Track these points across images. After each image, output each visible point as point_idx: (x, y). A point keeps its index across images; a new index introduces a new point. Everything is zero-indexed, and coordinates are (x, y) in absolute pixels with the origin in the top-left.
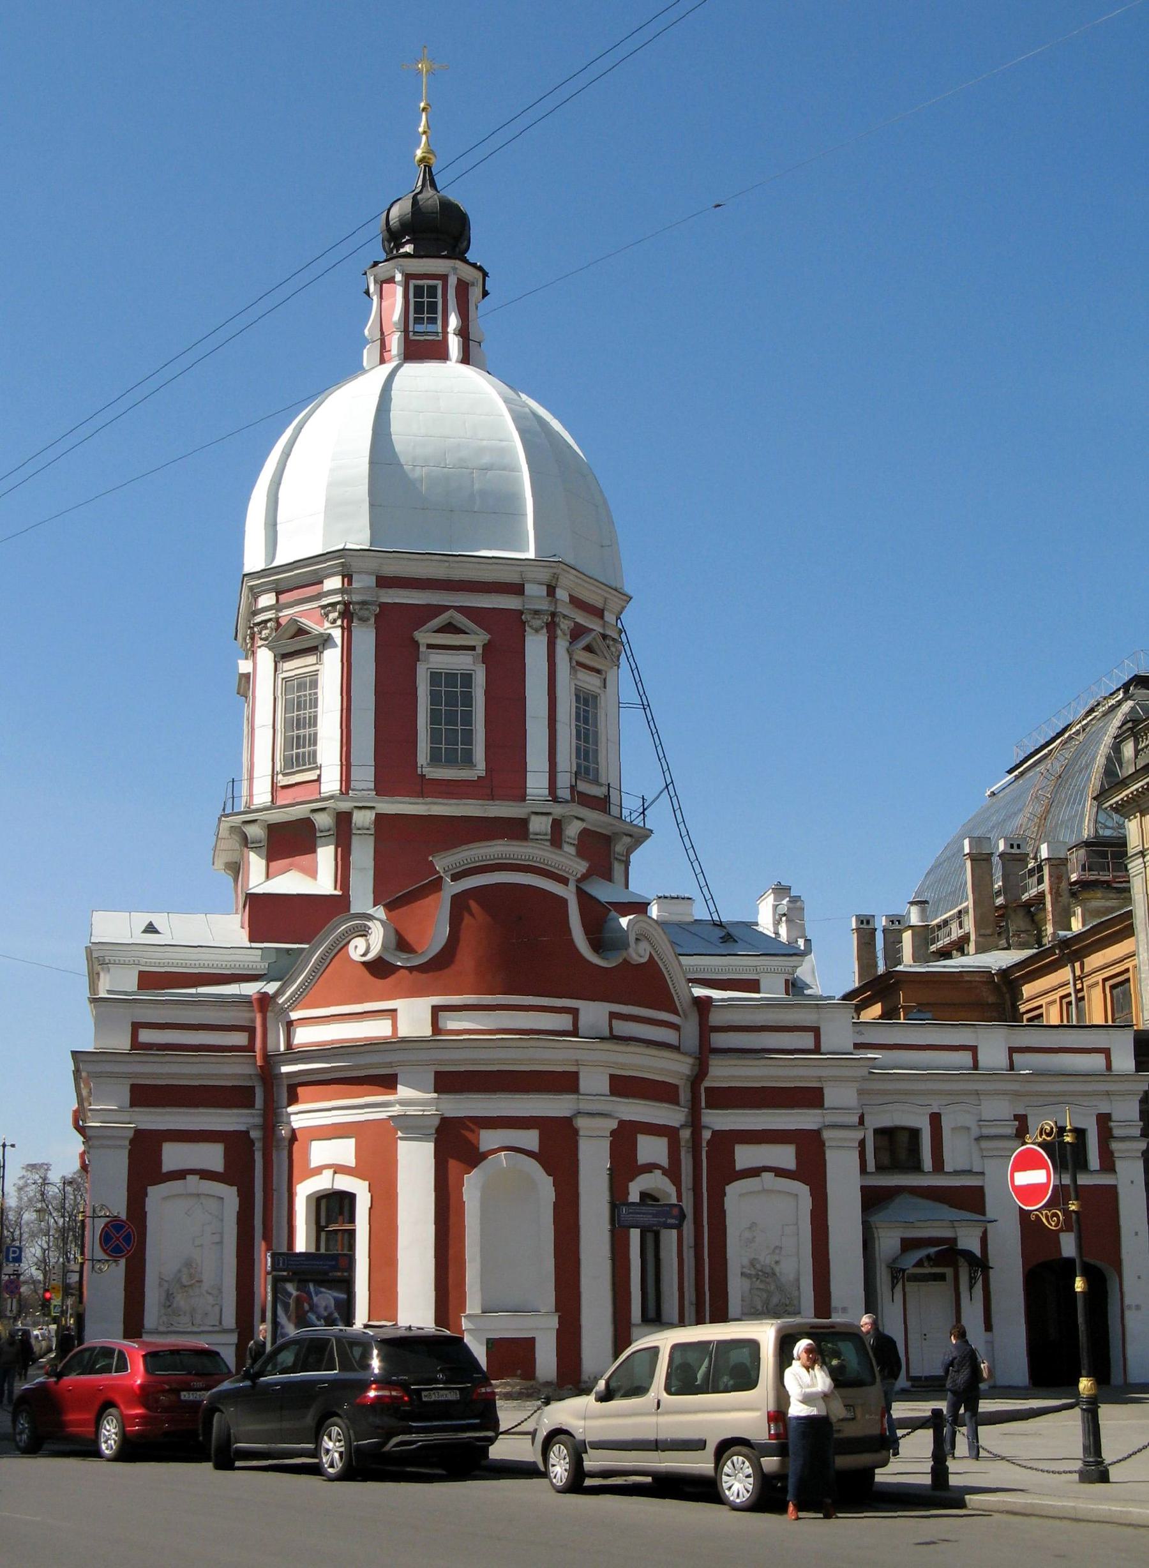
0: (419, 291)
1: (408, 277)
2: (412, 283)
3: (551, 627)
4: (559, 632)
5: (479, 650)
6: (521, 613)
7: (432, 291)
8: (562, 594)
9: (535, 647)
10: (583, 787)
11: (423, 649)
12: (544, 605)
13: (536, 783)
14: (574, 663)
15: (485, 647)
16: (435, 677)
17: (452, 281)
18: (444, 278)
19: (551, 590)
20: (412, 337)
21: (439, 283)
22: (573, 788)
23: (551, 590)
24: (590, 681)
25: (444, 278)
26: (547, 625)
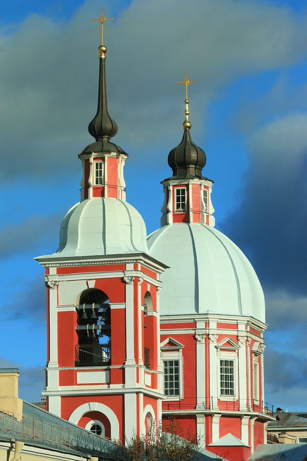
0: (178, 191)
1: (174, 186)
2: (176, 189)
5: (181, 350)
7: (183, 191)
8: (213, 325)
9: (200, 348)
12: (204, 332)
13: (201, 399)
14: (219, 350)
16: (165, 363)
18: (187, 186)
22: (219, 400)
23: (207, 324)
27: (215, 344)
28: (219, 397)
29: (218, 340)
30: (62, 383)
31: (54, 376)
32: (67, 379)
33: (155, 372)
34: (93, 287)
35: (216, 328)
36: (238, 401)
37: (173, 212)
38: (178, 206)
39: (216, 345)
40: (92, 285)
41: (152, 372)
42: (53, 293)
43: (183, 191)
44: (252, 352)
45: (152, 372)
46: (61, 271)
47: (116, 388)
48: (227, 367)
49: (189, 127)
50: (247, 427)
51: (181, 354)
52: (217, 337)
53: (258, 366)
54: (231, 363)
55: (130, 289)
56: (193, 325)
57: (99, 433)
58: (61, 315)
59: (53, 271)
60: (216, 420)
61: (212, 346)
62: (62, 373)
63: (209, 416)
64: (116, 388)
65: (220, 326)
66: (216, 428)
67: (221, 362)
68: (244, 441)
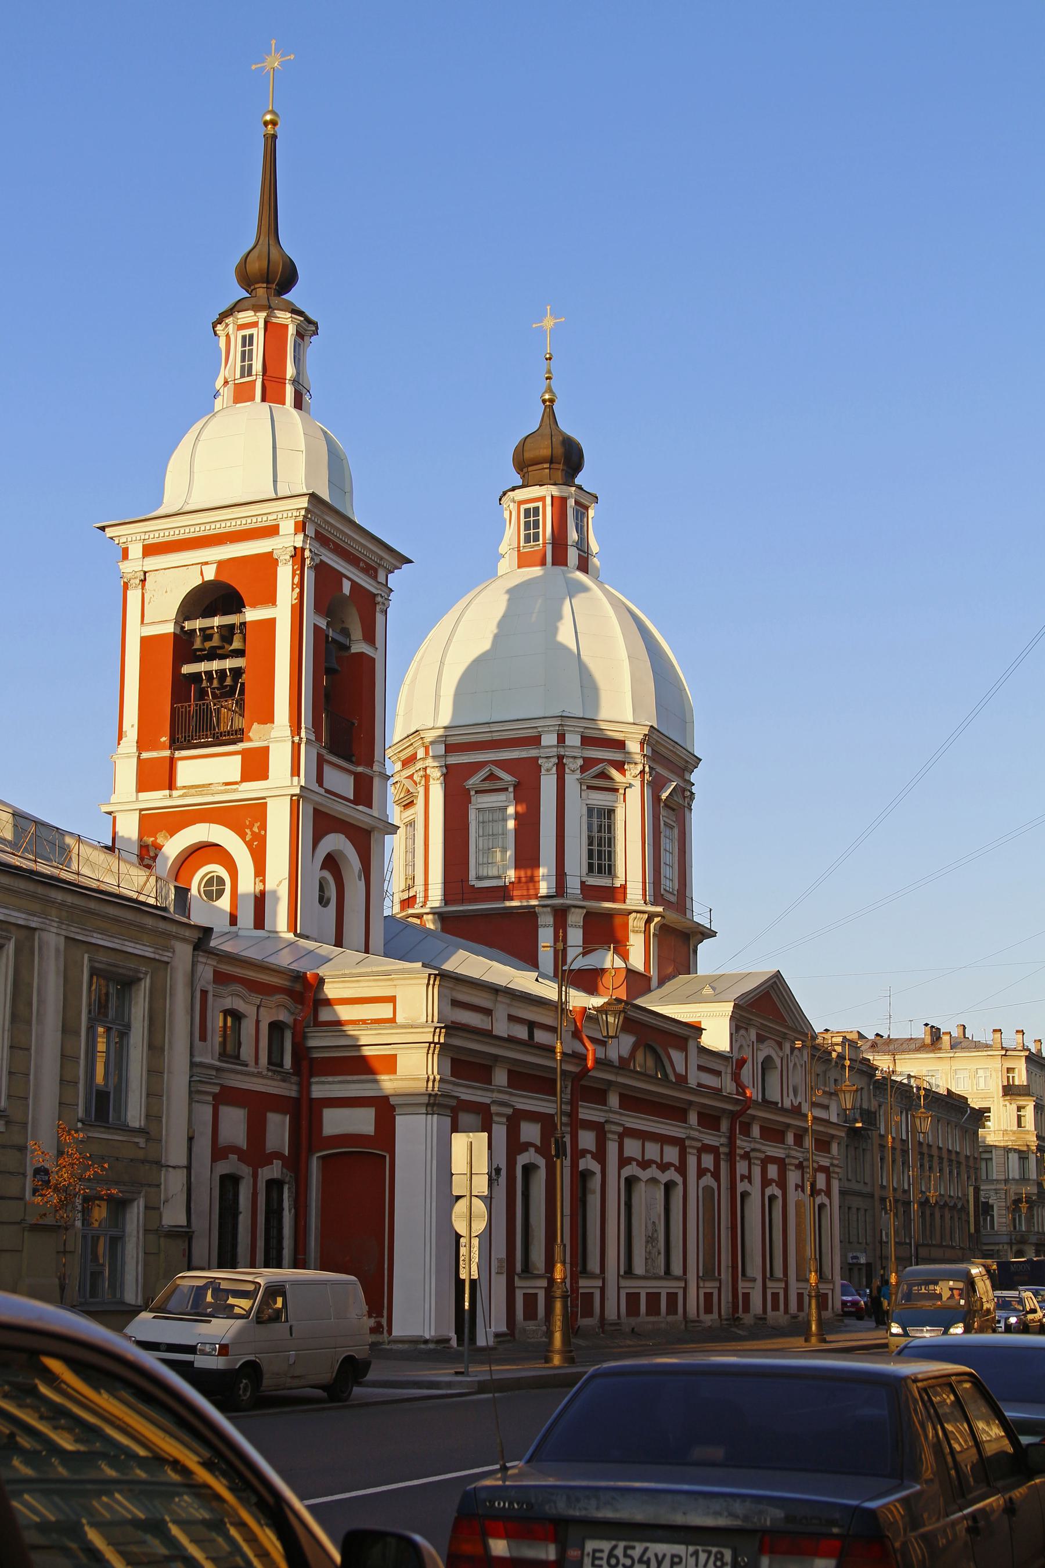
0: (527, 512)
2: (523, 507)
3: (561, 767)
4: (567, 770)
5: (511, 789)
6: (537, 758)
7: (536, 509)
8: (573, 740)
9: (548, 784)
10: (592, 881)
11: (472, 793)
15: (516, 787)
17: (549, 501)
19: (561, 738)
20: (522, 550)
21: (540, 504)
22: (583, 883)
23: (561, 738)
24: (599, 799)
25: (542, 499)
26: (557, 764)
27: (578, 775)
28: (584, 879)
29: (583, 769)
30: (143, 785)
31: (126, 772)
32: (156, 776)
33: (367, 771)
34: (212, 578)
35: (579, 744)
36: (624, 887)
37: (519, 547)
38: (527, 539)
39: (579, 777)
40: (210, 574)
41: (360, 769)
42: (134, 596)
43: (536, 509)
44: (656, 799)
45: (360, 769)
46: (150, 550)
47: (252, 790)
48: (603, 821)
49: (552, 401)
50: (641, 937)
51: (512, 795)
52: (580, 762)
53: (676, 831)
54: (611, 812)
55: (285, 575)
56: (535, 741)
57: (220, 893)
58: (145, 641)
59: (136, 551)
60: (575, 918)
61: (572, 781)
62: (142, 765)
63: (561, 916)
64: (252, 790)
65: (587, 741)
66: (575, 936)
67: (590, 810)
68: (637, 960)
